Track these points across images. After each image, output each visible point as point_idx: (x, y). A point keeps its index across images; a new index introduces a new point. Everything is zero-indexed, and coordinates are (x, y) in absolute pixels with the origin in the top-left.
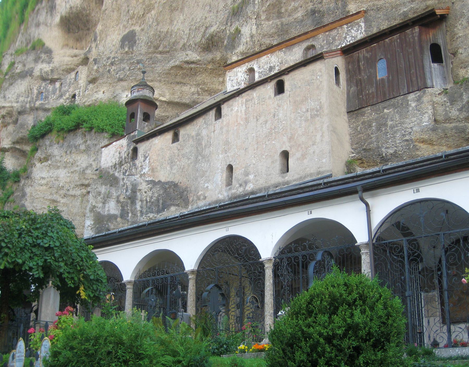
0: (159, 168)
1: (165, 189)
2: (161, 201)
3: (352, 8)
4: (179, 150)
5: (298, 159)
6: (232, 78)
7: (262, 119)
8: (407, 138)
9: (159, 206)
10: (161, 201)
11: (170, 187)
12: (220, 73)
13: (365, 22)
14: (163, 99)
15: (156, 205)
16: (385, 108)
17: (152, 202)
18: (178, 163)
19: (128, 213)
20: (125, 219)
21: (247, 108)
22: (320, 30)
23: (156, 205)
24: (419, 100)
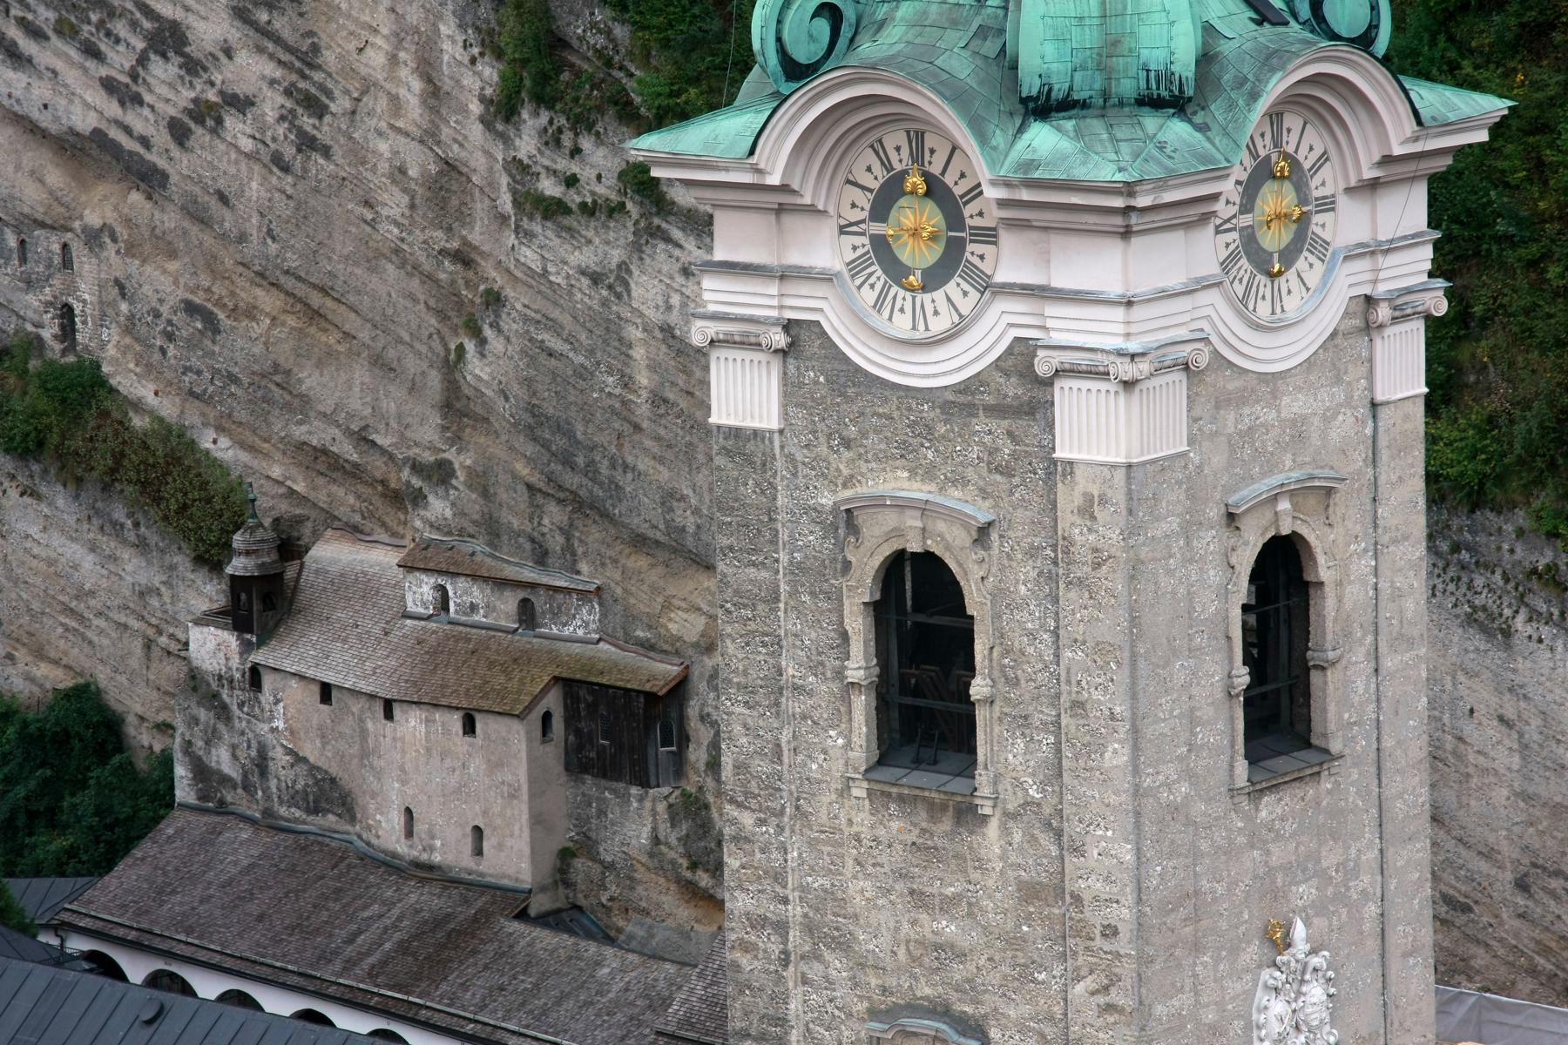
5: (494, 847)
7: (448, 762)
8: (624, 849)
13: (601, 605)
16: (606, 789)
21: (428, 733)
24: (641, 800)
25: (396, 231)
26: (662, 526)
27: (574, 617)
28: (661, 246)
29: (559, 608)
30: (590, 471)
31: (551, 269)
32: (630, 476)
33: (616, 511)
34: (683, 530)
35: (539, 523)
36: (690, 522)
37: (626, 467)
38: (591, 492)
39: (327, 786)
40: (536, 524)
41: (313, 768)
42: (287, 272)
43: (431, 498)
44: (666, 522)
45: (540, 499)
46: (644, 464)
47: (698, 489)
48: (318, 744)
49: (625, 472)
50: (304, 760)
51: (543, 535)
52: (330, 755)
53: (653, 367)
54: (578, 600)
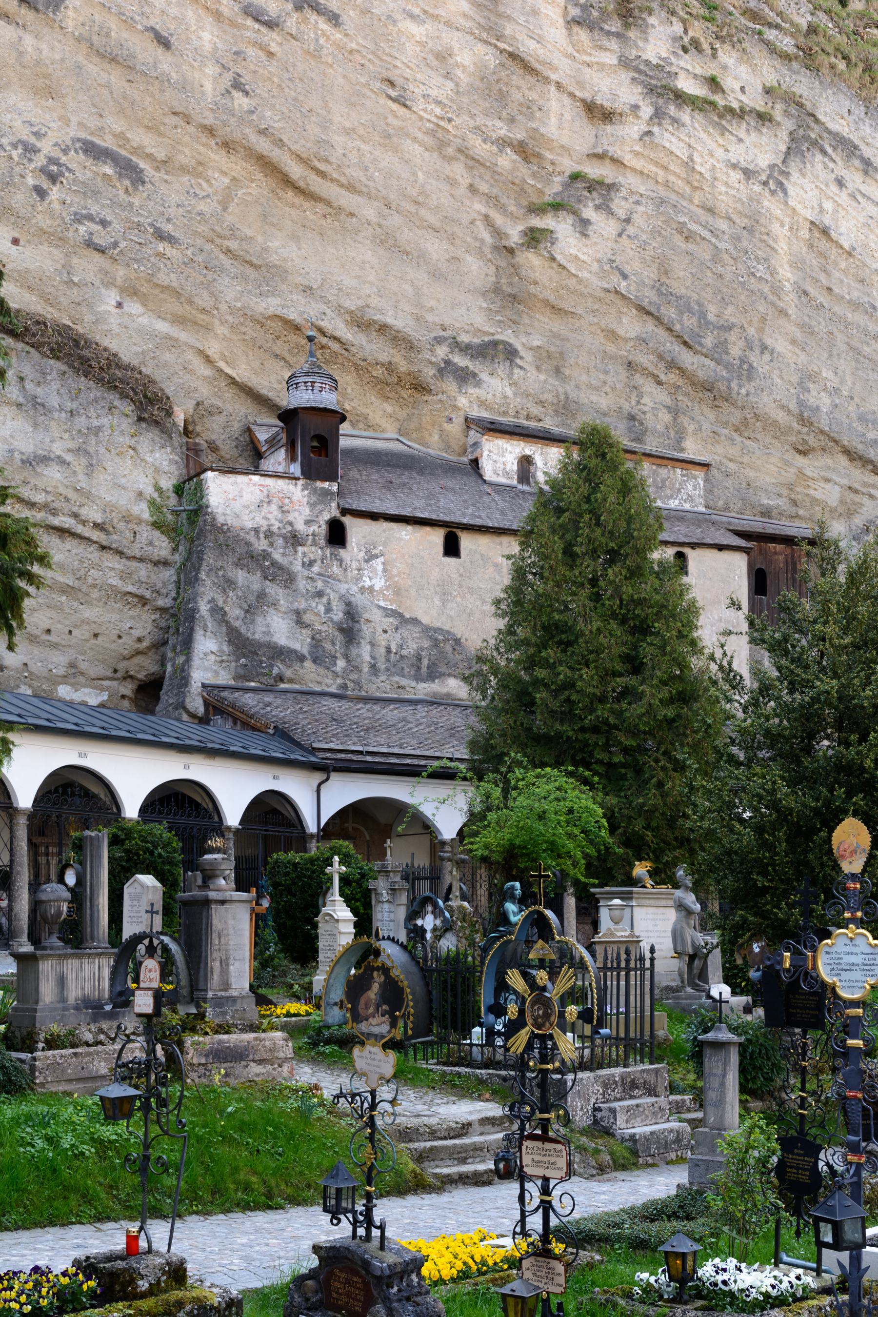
0: (413, 592)
1: (436, 643)
2: (425, 662)
3: (692, 449)
4: (461, 575)
6: (495, 457)
9: (419, 668)
10: (425, 662)
11: (446, 640)
12: (390, 395)
14: (228, 370)
15: (412, 665)
17: (402, 657)
18: (459, 599)
19: (335, 657)
20: (328, 668)
22: (651, 459)
23: (412, 665)
25: (438, 111)
26: (793, 406)
27: (679, 490)
28: (819, 157)
29: (663, 481)
30: (718, 353)
31: (697, 158)
32: (767, 357)
33: (743, 391)
34: (818, 408)
35: (638, 402)
36: (825, 402)
37: (764, 348)
38: (715, 371)
39: (448, 649)
40: (633, 403)
41: (428, 631)
42: (263, 132)
43: (484, 376)
44: (801, 403)
45: (639, 379)
46: (780, 345)
47: (840, 373)
48: (437, 602)
49: (762, 353)
50: (415, 621)
51: (644, 413)
52: (452, 613)
53: (794, 265)
54: (682, 476)
